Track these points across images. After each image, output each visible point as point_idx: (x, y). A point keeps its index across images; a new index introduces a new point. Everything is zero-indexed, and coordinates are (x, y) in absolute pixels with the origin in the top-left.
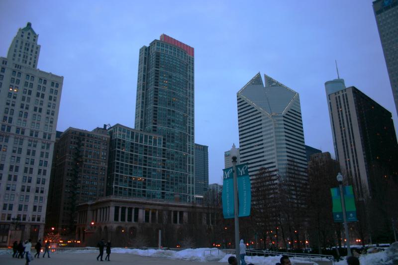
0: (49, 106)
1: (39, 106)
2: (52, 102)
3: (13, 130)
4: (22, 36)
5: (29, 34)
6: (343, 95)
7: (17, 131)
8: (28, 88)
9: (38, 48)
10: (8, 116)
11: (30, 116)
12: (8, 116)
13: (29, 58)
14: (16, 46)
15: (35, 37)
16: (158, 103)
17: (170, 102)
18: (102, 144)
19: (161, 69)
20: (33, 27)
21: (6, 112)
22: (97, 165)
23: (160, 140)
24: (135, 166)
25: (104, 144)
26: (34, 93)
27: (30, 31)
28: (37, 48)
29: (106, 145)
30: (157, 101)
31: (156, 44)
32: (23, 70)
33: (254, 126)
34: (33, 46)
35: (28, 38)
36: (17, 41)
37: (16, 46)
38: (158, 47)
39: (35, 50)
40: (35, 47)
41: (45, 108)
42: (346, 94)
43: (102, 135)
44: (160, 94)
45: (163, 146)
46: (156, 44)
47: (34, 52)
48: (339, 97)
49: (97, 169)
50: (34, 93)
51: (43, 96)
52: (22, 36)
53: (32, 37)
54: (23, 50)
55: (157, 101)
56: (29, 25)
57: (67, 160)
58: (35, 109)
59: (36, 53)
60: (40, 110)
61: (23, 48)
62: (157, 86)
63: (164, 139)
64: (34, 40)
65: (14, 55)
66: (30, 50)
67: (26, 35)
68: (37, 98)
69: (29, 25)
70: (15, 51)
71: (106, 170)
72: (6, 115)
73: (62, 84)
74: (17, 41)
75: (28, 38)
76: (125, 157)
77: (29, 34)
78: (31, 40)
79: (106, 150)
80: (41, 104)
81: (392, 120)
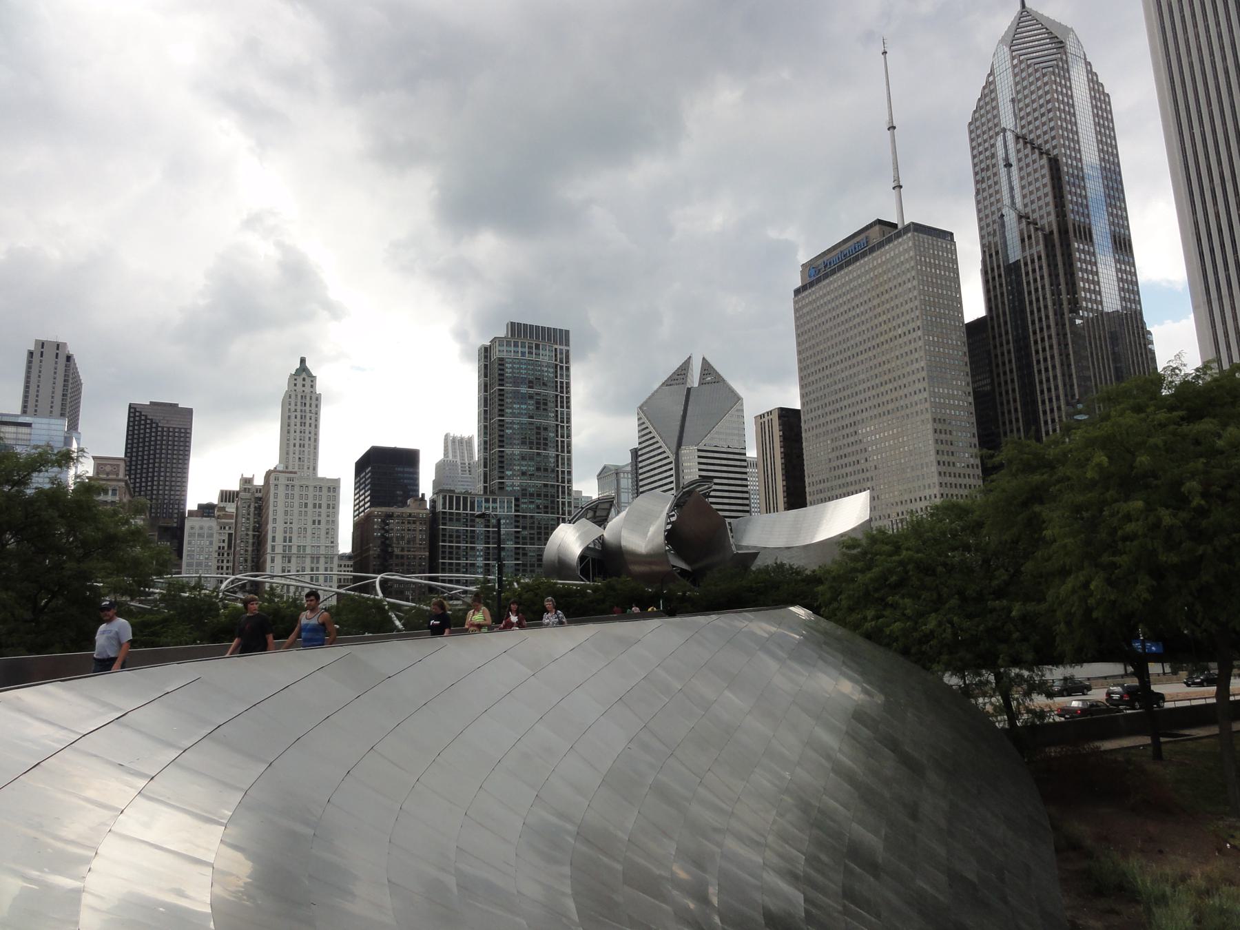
0: (328, 516)
1: (317, 518)
2: (331, 510)
3: (294, 550)
4: (295, 385)
5: (304, 379)
6: (768, 421)
7: (299, 551)
8: (304, 501)
9: (318, 398)
10: (288, 535)
11: (309, 531)
12: (288, 535)
13: (308, 418)
14: (290, 404)
15: (312, 381)
16: (504, 444)
17: (526, 438)
18: (418, 523)
19: (508, 387)
20: (308, 364)
21: (285, 532)
22: (413, 553)
23: (509, 502)
24: (471, 547)
25: (421, 523)
26: (310, 506)
27: (304, 375)
28: (317, 400)
29: (425, 524)
30: (503, 441)
31: (497, 343)
32: (296, 483)
33: (655, 469)
34: (311, 399)
35: (304, 386)
36: (290, 397)
37: (290, 404)
38: (501, 349)
39: (314, 403)
40: (314, 399)
41: (323, 519)
42: (771, 420)
43: (419, 511)
44: (507, 428)
45: (516, 511)
46: (497, 343)
47: (313, 406)
48: (764, 422)
49: (414, 558)
50: (310, 506)
51: (320, 507)
52: (295, 385)
53: (308, 381)
54: (299, 408)
55: (503, 441)
56: (303, 361)
57: (371, 552)
58: (314, 522)
59: (317, 406)
60: (319, 522)
61: (299, 404)
62: (503, 416)
63: (517, 500)
64: (312, 386)
65: (289, 417)
66: (308, 405)
67: (300, 382)
68: (314, 510)
69: (303, 361)
70: (289, 426)
71: (427, 559)
72: (285, 535)
73: (339, 487)
74: (290, 397)
75: (304, 386)
76: (454, 536)
77: (304, 379)
78: (307, 389)
79: (425, 531)
80: (319, 515)
81: (1153, 353)
